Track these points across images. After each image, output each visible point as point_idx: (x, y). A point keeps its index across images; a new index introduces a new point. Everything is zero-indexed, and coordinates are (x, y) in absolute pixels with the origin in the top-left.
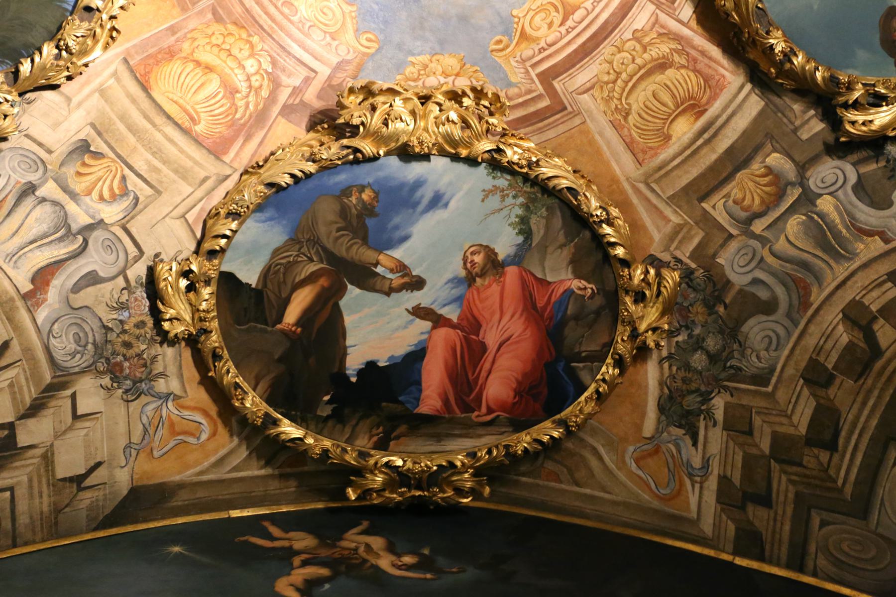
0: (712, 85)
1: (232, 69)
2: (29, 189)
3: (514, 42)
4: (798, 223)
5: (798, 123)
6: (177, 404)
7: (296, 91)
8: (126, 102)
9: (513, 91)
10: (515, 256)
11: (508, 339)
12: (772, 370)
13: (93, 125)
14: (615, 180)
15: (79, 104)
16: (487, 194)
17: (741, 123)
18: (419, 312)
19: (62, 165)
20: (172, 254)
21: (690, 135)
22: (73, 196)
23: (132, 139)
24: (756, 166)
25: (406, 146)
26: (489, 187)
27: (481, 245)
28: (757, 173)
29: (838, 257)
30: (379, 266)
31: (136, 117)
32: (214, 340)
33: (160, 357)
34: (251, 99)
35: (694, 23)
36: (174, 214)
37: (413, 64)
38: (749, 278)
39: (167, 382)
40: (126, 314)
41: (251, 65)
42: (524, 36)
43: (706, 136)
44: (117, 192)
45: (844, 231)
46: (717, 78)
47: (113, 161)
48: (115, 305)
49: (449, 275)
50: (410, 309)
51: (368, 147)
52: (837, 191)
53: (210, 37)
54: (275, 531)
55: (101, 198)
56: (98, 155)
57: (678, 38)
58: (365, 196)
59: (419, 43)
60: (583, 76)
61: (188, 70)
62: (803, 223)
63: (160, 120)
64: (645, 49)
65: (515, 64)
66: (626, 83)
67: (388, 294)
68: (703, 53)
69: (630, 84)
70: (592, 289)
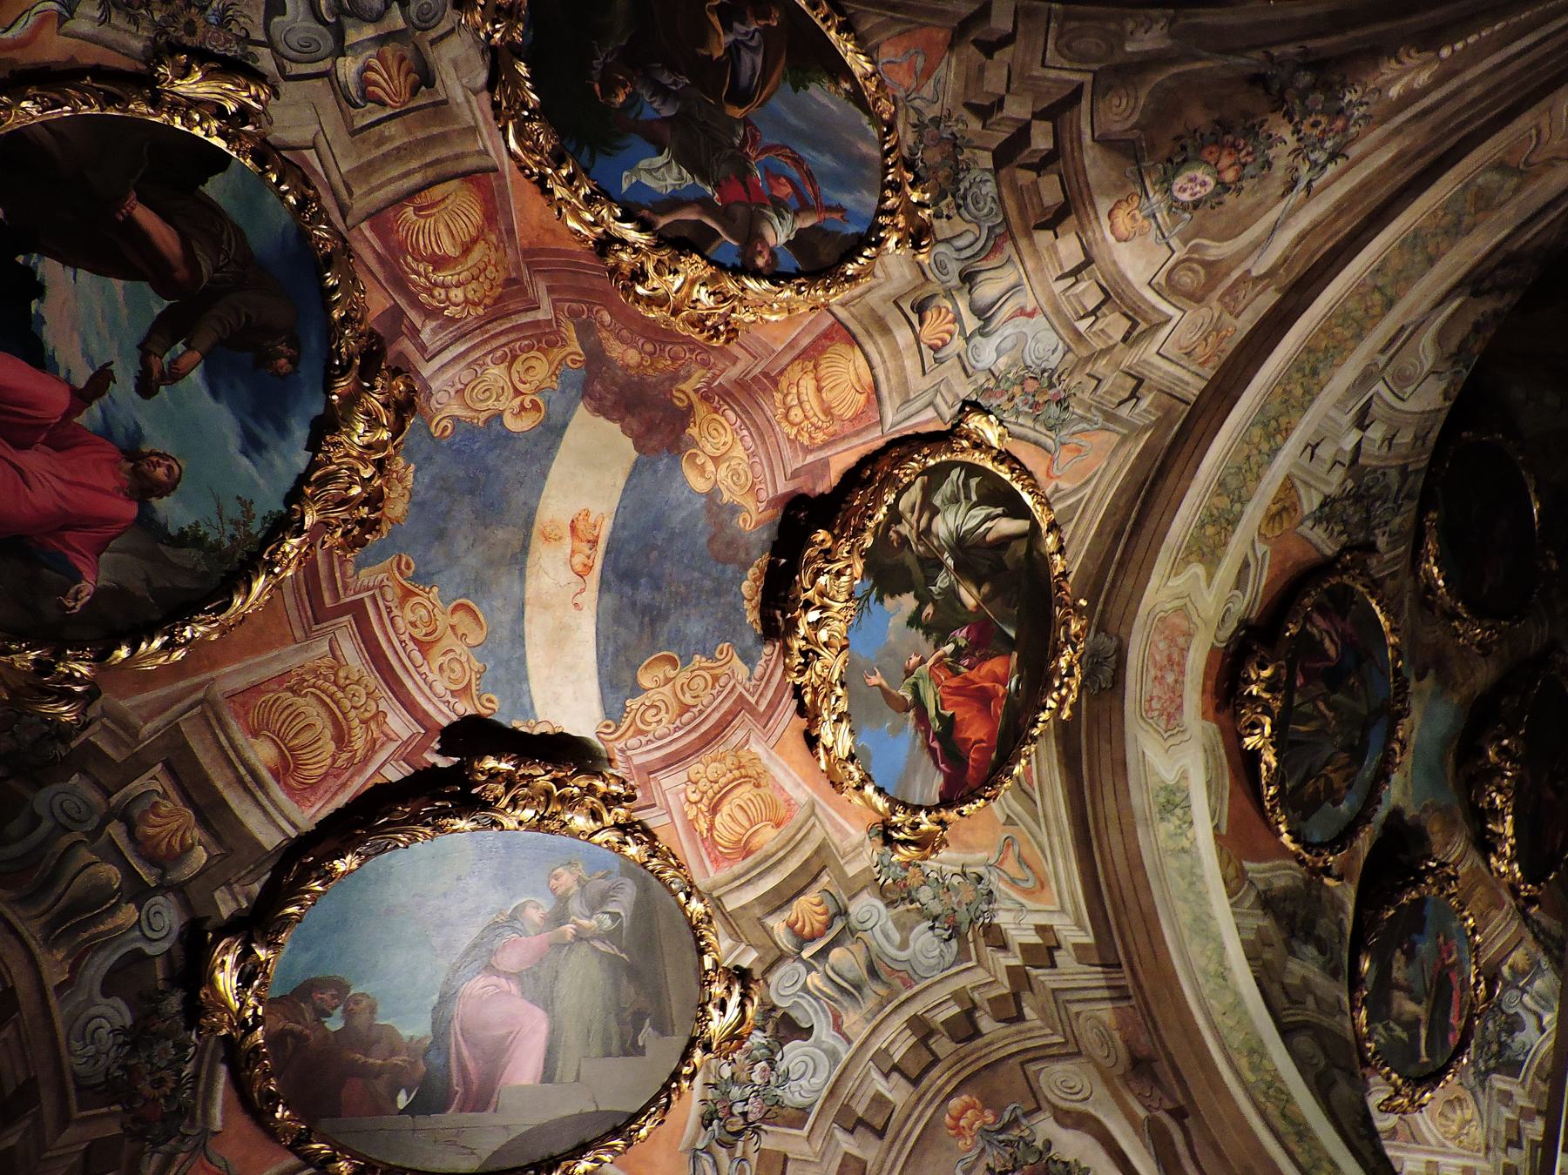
0: (303, 792)
1: (459, 274)
3: (404, 582)
4: (110, 879)
5: (237, 888)
6: (50, 16)
7: (415, 332)
8: (458, 149)
9: (350, 569)
10: (152, 520)
11: (26, 482)
13: (445, 102)
14: (214, 665)
15: (468, 101)
16: (246, 505)
17: (253, 821)
18: (102, 378)
19: (416, 46)
20: (272, 112)
21: (253, 760)
22: (381, 40)
23: (420, 135)
25: (334, 428)
26: (255, 509)
27: (178, 480)
28: (188, 834)
29: (51, 927)
30: (184, 348)
31: (443, 152)
32: (140, 109)
33: (134, 29)
34: (423, 280)
35: (379, 780)
36: (321, 138)
37: (406, 468)
38: (41, 810)
39: (92, 19)
40: (212, 20)
41: (457, 295)
42: (408, 594)
43: (248, 778)
44: (371, 88)
45: (85, 936)
46: (312, 799)
47: (404, 103)
48: (230, 13)
49: (147, 430)
50: (113, 367)
51: (343, 384)
52: (141, 930)
53: (495, 266)
55: (368, 68)
56: (414, 92)
57: (366, 760)
58: (283, 361)
59: (426, 481)
60: (350, 650)
61: (471, 229)
62: (109, 884)
63: (431, 173)
64: (364, 722)
65: (379, 578)
66: (331, 696)
67: (141, 347)
68: (344, 785)
69: (328, 700)
70: (74, 608)
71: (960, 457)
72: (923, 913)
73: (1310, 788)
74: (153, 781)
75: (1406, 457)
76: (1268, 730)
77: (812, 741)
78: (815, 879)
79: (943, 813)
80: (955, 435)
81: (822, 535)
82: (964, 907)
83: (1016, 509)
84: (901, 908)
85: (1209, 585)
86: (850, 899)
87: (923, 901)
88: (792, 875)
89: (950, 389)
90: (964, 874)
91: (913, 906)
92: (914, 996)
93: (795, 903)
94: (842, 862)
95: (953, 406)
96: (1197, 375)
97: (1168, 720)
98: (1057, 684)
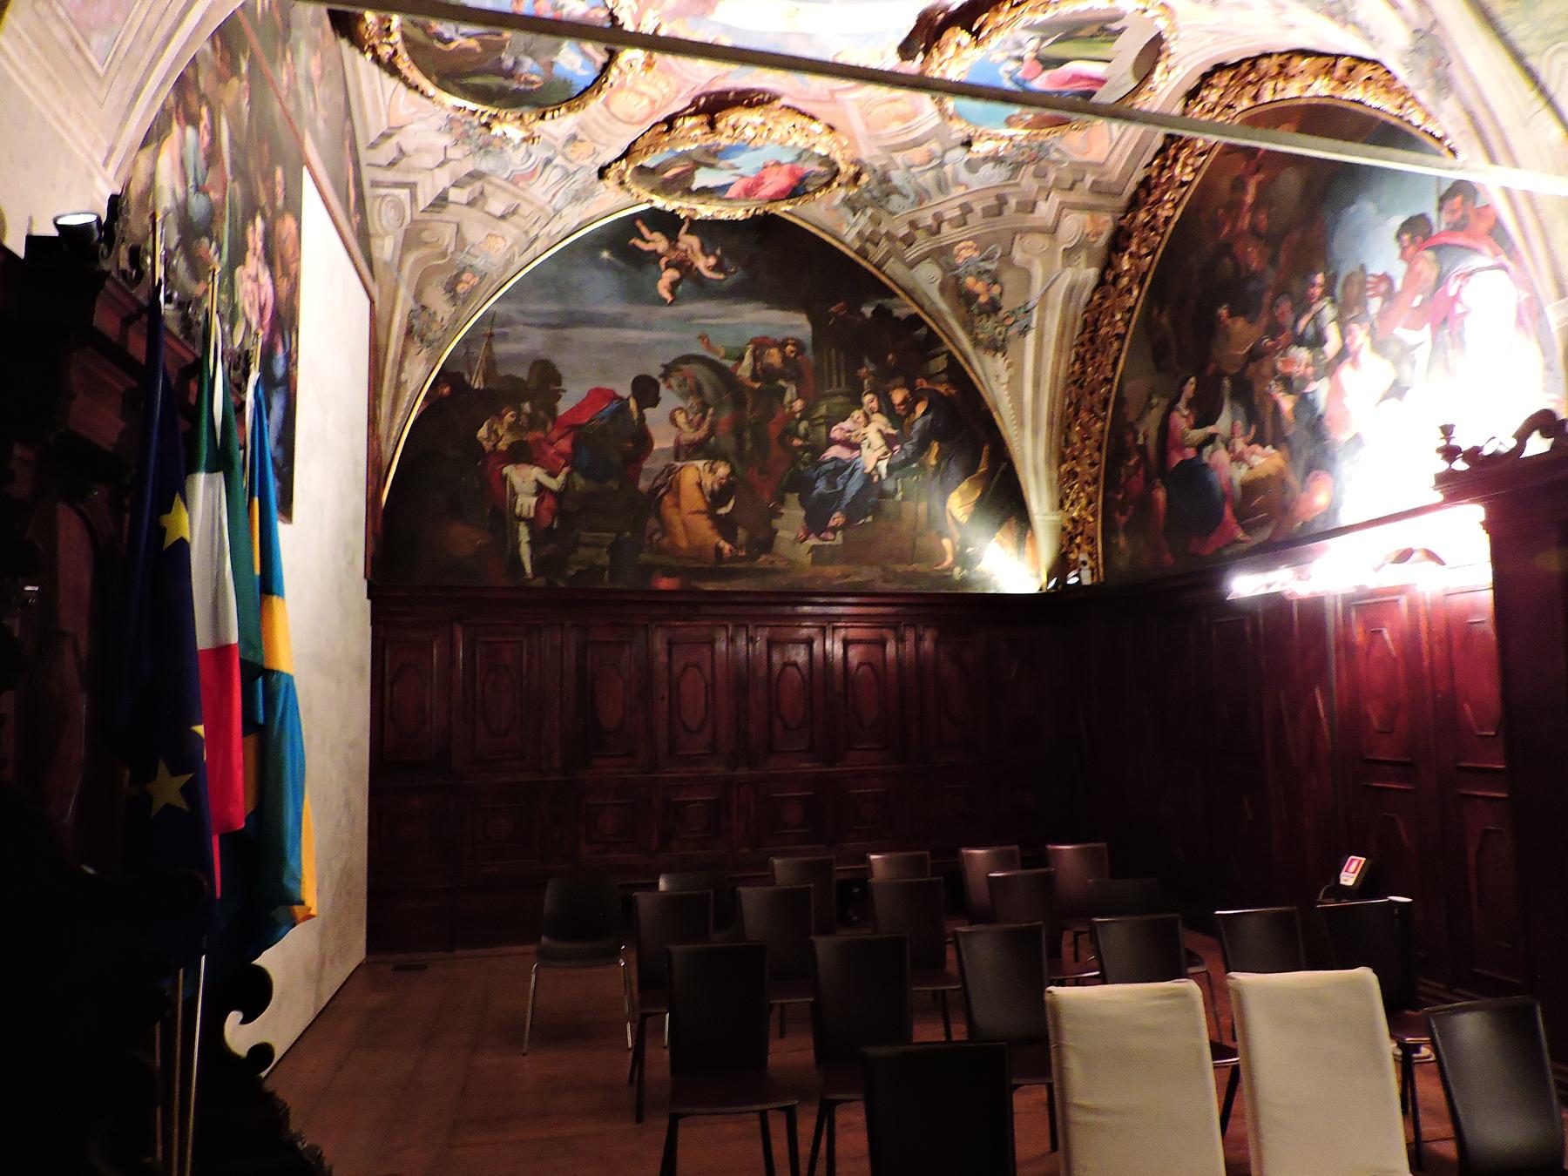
2: (548, 162)
12: (895, 214)
13: (578, 124)
17: (925, 128)
22: (571, 162)
24: (925, 147)
31: (601, 119)
54: (644, 230)
56: (582, 141)
74: (899, 158)
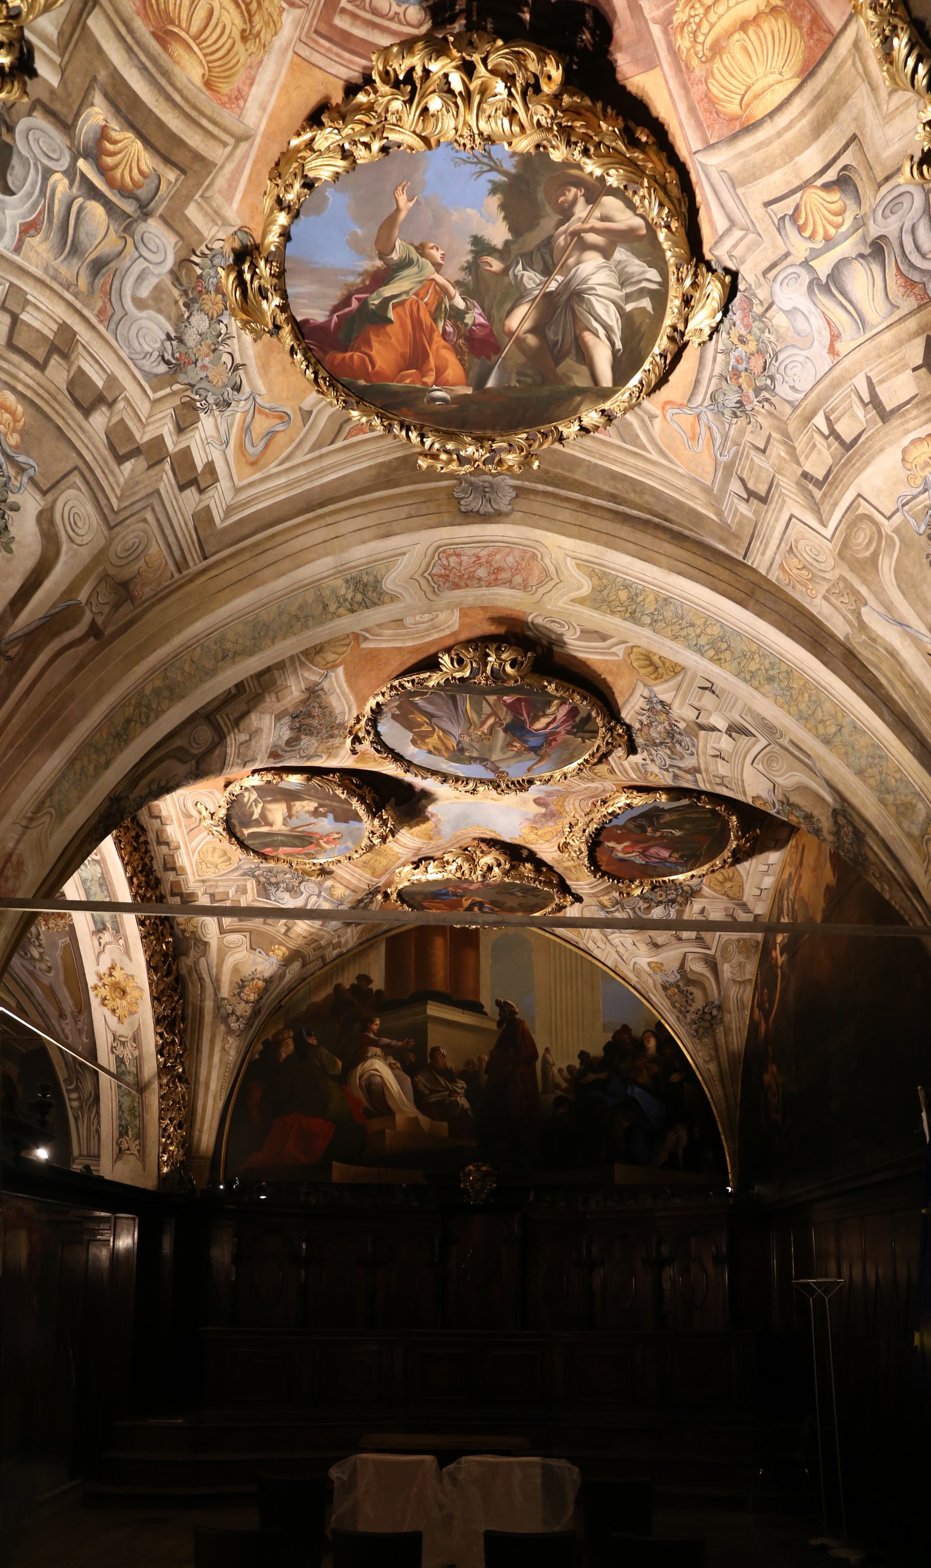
71: (672, 279)
72: (181, 322)
73: (421, 719)
75: (707, 770)
76: (458, 675)
77: (315, 119)
78: (168, 161)
79: (287, 329)
80: (697, 266)
81: (557, 74)
82: (203, 375)
83: (622, 371)
84: (176, 293)
85: (573, 601)
86: (161, 217)
87: (192, 319)
88: (161, 125)
89: (751, 248)
90: (235, 368)
91: (183, 309)
92: (93, 327)
93: (130, 135)
94: (197, 197)
95: (731, 256)
96: (772, 564)
97: (441, 576)
98: (450, 446)
